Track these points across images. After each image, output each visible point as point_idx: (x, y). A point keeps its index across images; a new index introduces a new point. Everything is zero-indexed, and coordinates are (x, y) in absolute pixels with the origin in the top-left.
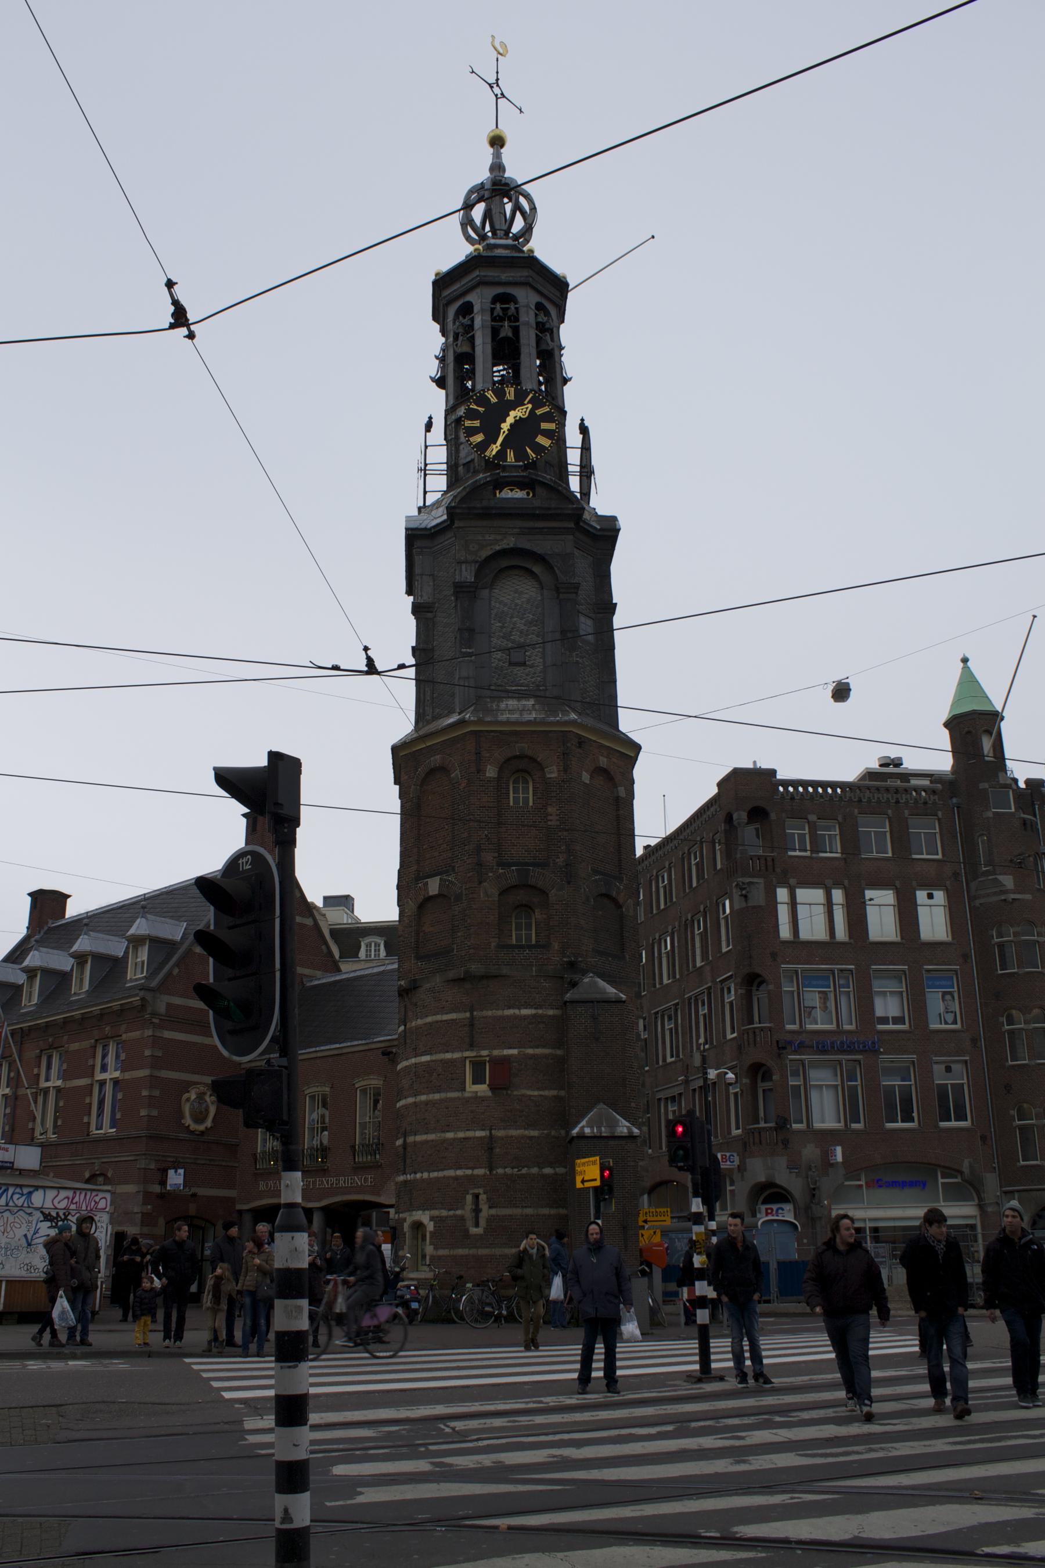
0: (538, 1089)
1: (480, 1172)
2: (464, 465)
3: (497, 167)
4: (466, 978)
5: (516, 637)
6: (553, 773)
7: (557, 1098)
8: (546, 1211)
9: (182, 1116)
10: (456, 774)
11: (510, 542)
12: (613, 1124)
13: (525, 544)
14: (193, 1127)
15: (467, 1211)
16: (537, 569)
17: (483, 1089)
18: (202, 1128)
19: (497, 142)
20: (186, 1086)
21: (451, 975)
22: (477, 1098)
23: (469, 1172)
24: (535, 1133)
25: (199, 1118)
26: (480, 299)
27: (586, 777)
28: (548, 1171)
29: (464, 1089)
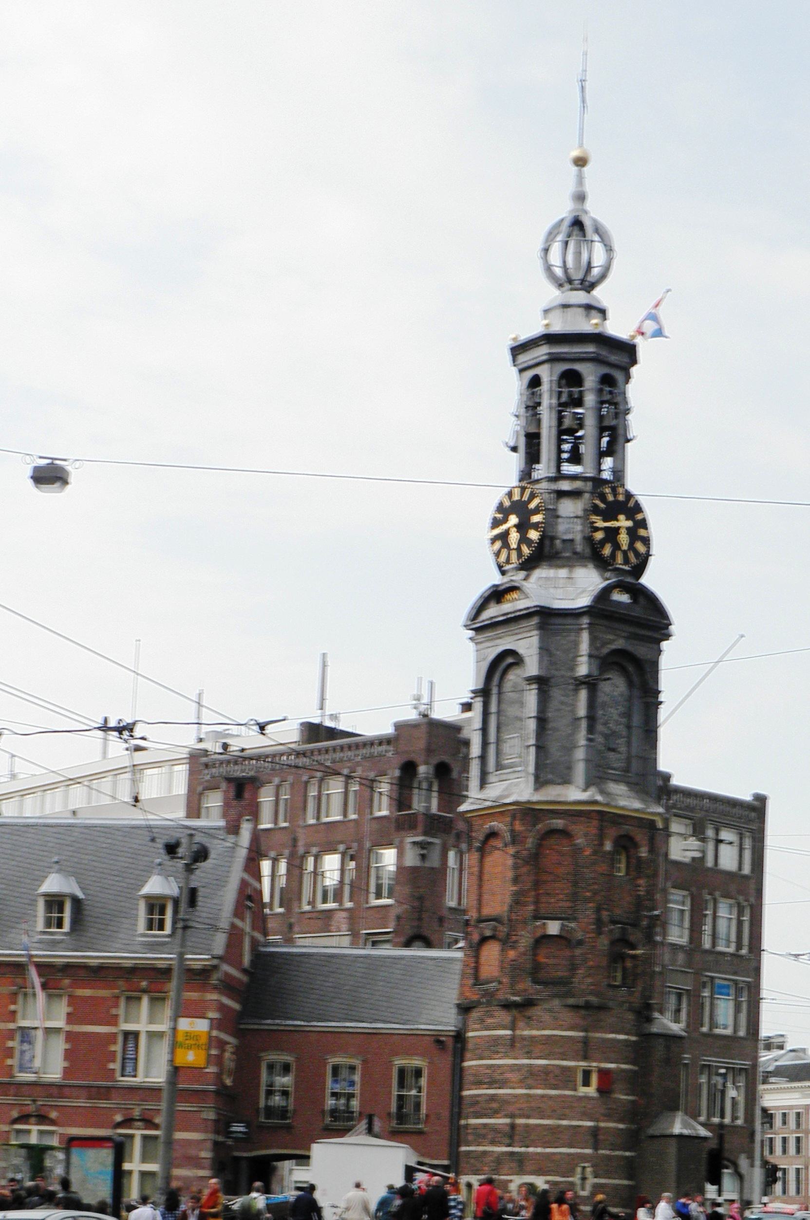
0: (627, 1094)
1: (588, 1151)
2: (564, 541)
3: (581, 198)
4: (588, 1006)
6: (644, 853)
7: (633, 1102)
8: (626, 1182)
10: (580, 841)
11: (620, 644)
15: (576, 1179)
16: (631, 669)
17: (591, 1091)
19: (581, 162)
21: (571, 1001)
22: (587, 1098)
23: (579, 1151)
24: (621, 1126)
28: (627, 1154)
29: (575, 1090)
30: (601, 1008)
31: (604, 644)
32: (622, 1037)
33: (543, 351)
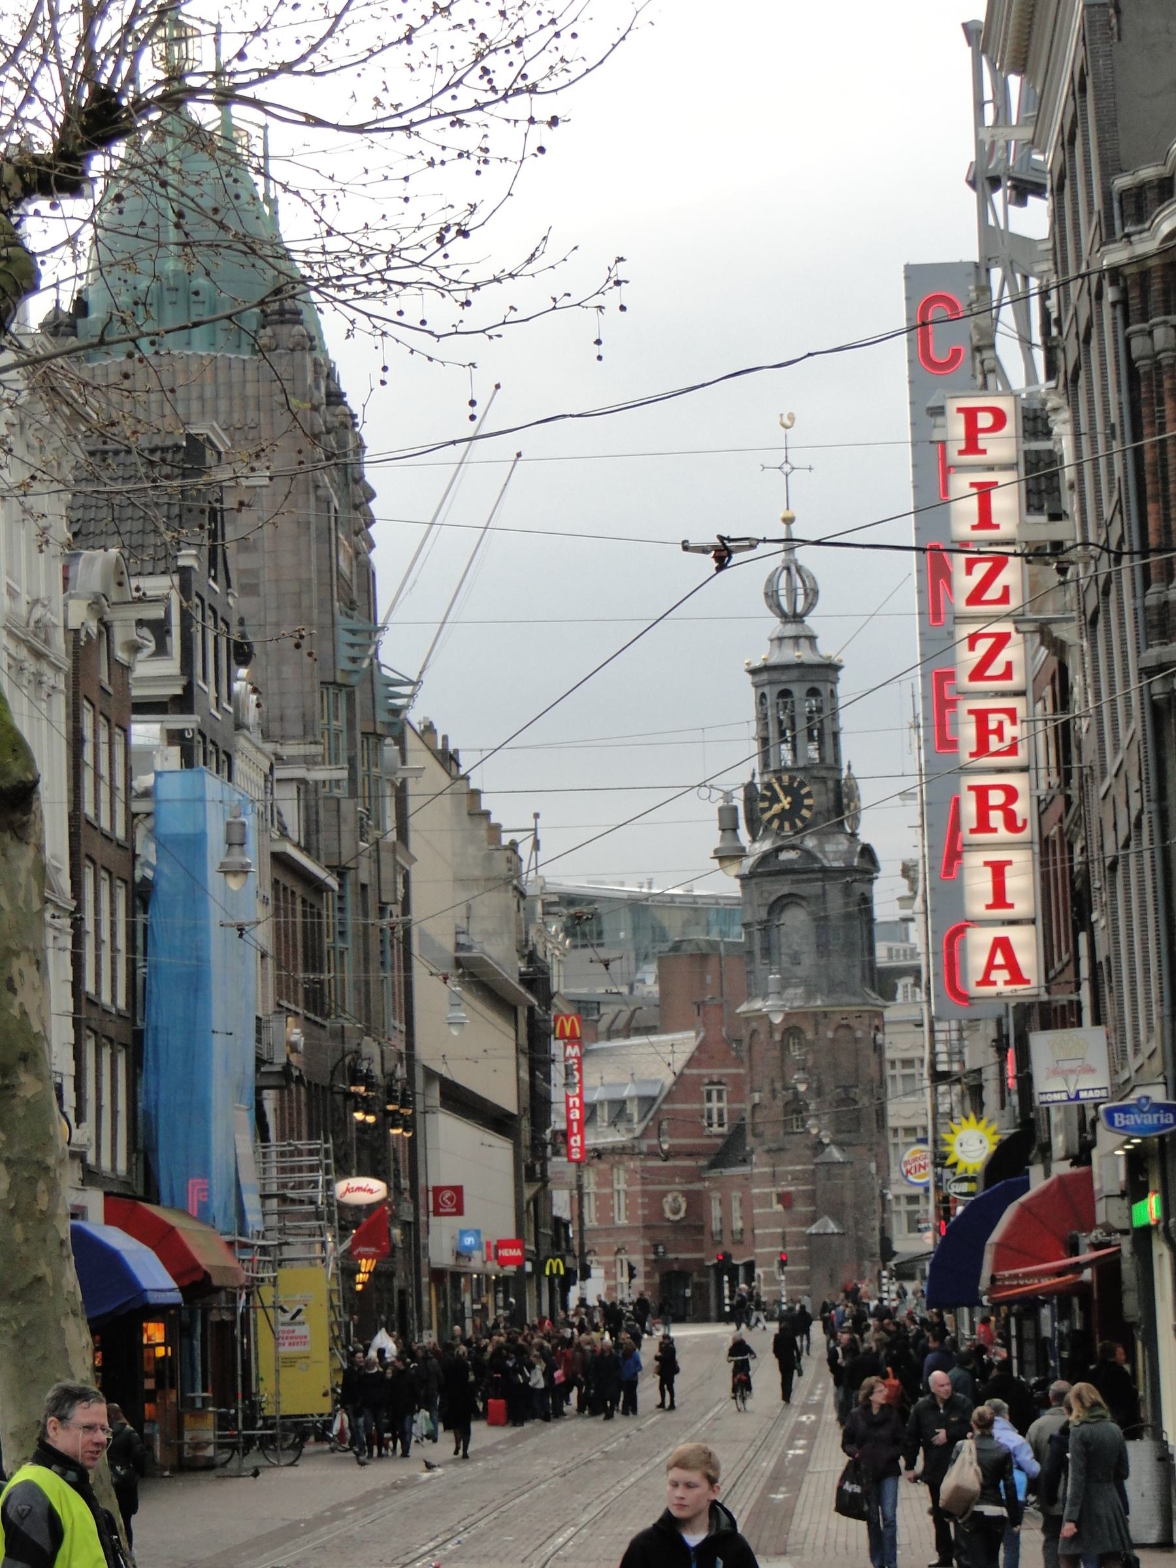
5: (795, 947)
6: (810, 1035)
9: (663, 1210)
10: (762, 1036)
11: (786, 890)
12: (826, 1226)
13: (794, 891)
14: (672, 1217)
18: (677, 1218)
20: (664, 1194)
21: (766, 1147)
22: (777, 1212)
25: (676, 1211)
26: (771, 692)
27: (830, 1034)
30: (780, 1150)
31: (770, 894)
32: (799, 1168)
33: (765, 677)
